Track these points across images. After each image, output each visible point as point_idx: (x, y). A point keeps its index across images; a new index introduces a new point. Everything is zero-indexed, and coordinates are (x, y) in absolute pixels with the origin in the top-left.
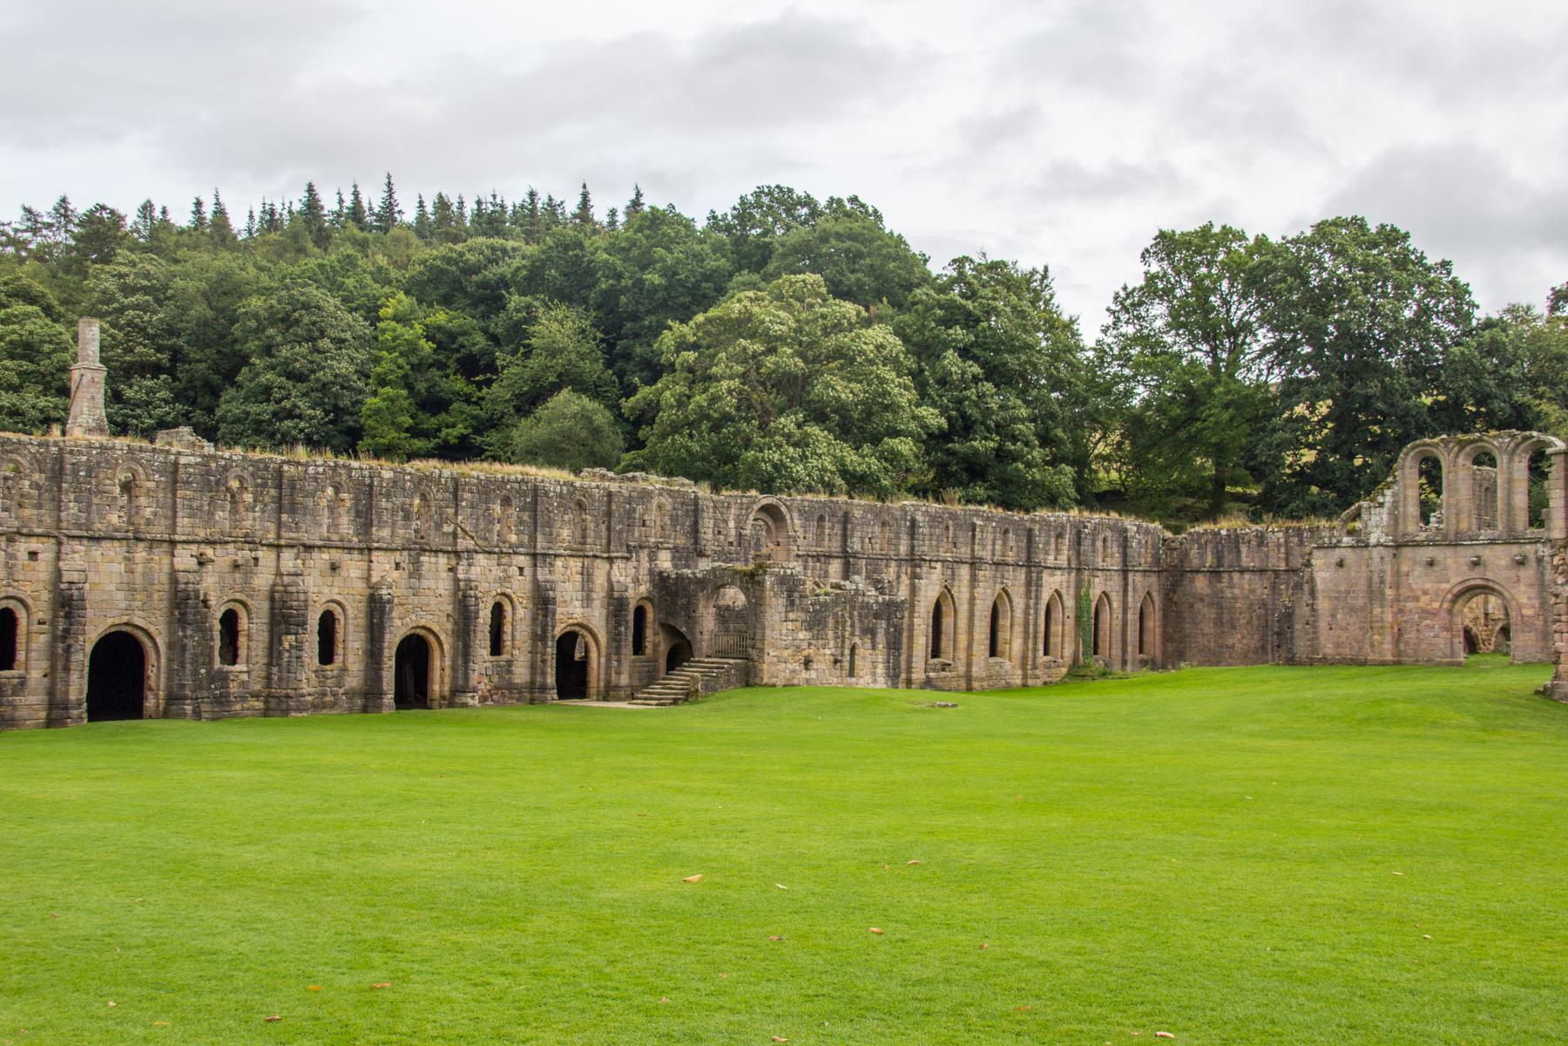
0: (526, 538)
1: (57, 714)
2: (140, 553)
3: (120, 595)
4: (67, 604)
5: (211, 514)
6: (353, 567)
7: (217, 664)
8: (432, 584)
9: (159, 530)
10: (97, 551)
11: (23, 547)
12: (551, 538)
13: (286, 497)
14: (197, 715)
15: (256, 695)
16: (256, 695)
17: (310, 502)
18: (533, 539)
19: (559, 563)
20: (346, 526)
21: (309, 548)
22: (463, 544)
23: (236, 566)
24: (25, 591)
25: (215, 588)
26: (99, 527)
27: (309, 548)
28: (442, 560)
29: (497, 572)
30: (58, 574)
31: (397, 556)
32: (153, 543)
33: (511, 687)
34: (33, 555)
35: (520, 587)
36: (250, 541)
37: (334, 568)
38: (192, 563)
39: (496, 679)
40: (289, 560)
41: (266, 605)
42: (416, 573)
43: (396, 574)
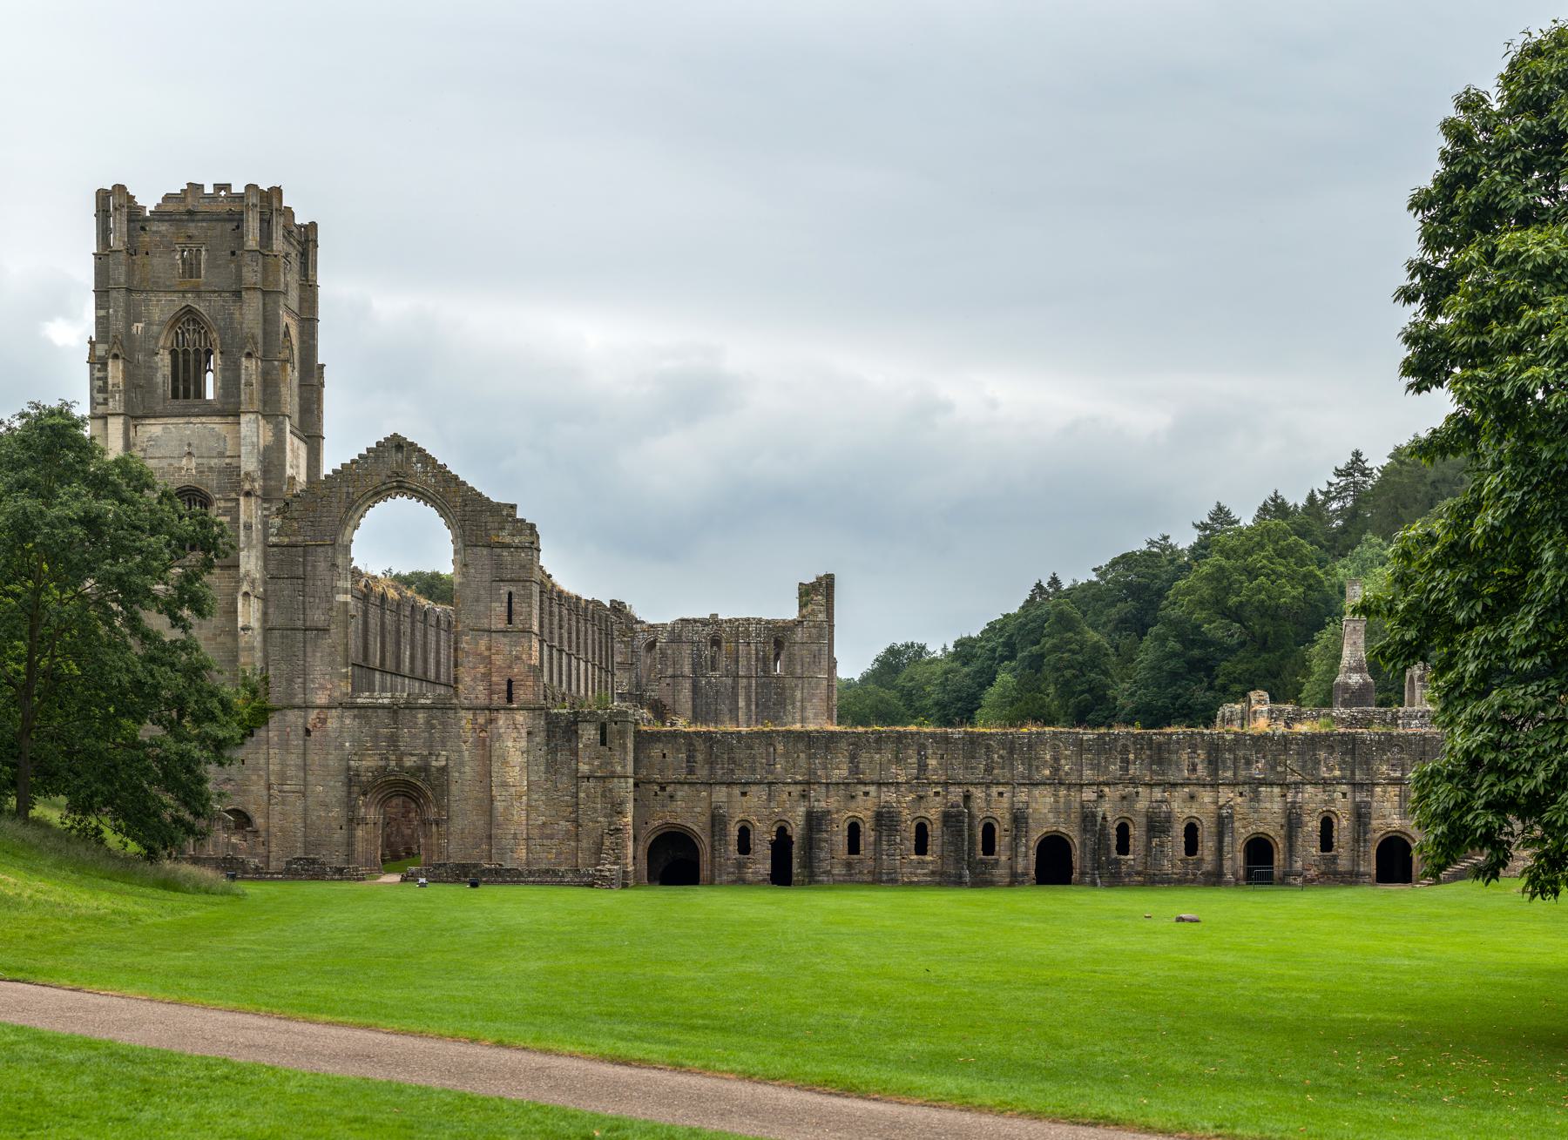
0: (1348, 773)
1: (1015, 881)
2: (1063, 792)
3: (1050, 815)
4: (1019, 819)
5: (1107, 767)
6: (1206, 796)
7: (1114, 854)
8: (1268, 805)
9: (1073, 779)
10: (1036, 792)
11: (994, 790)
12: (1369, 771)
13: (1160, 755)
14: (1094, 884)
15: (1139, 873)
16: (1139, 873)
17: (1174, 757)
18: (1353, 773)
19: (1378, 789)
20: (1201, 771)
21: (1174, 785)
22: (1290, 779)
23: (1124, 798)
24: (998, 814)
25: (1109, 809)
26: (1037, 777)
27: (1174, 785)
28: (1277, 790)
29: (1322, 796)
30: (1013, 803)
31: (1241, 789)
32: (1070, 786)
33: (1336, 873)
34: (1001, 794)
35: (1342, 805)
36: (1134, 782)
37: (1192, 797)
38: (1093, 796)
39: (1323, 867)
40: (1158, 794)
41: (1144, 820)
42: (1256, 798)
43: (1239, 800)
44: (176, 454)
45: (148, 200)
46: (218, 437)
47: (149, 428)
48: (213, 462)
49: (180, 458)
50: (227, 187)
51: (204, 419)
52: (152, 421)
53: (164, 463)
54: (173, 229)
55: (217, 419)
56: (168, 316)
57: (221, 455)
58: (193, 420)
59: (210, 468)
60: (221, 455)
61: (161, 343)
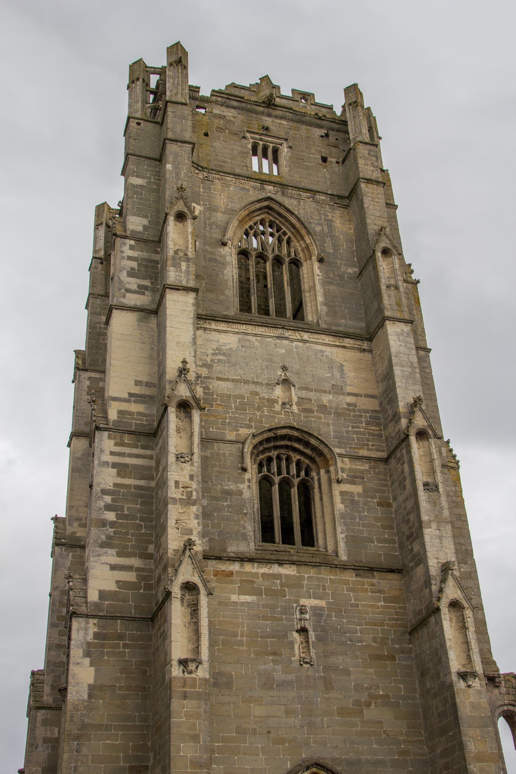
44: (264, 378)
45: (206, 77)
46: (331, 365)
47: (215, 336)
48: (326, 399)
49: (271, 386)
50: (306, 96)
51: (306, 336)
52: (222, 326)
53: (244, 390)
54: (241, 117)
55: (327, 339)
56: (238, 206)
57: (338, 390)
58: (287, 334)
59: (323, 408)
60: (338, 390)
61: (230, 234)
